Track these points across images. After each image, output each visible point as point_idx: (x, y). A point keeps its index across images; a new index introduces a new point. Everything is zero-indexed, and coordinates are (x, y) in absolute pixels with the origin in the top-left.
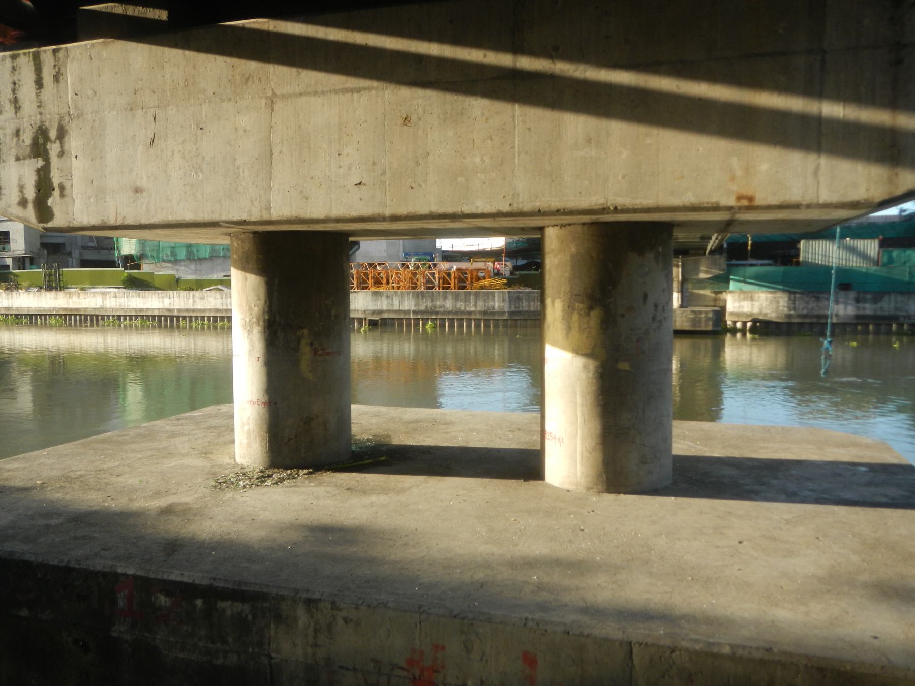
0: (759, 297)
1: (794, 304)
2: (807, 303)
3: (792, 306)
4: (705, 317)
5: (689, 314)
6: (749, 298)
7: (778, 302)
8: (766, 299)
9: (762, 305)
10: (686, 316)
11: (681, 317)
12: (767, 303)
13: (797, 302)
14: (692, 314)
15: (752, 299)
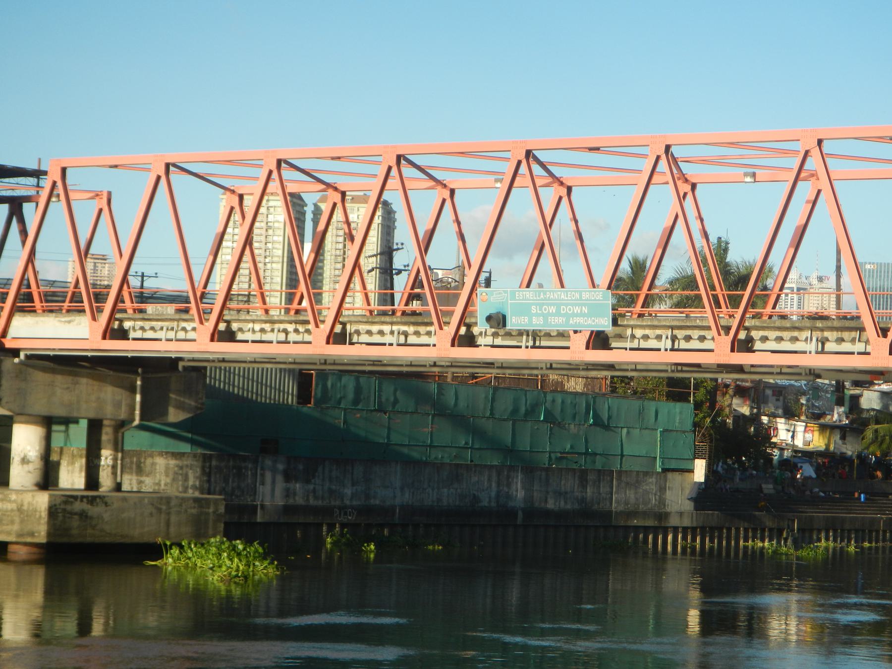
0: (153, 464)
1: (209, 481)
2: (226, 481)
3: (206, 486)
4: (214, 512)
5: (191, 508)
6: (134, 466)
7: (186, 479)
8: (167, 468)
9: (159, 484)
10: (186, 511)
11: (179, 513)
12: (168, 480)
13: (212, 480)
14: (194, 508)
15: (140, 471)
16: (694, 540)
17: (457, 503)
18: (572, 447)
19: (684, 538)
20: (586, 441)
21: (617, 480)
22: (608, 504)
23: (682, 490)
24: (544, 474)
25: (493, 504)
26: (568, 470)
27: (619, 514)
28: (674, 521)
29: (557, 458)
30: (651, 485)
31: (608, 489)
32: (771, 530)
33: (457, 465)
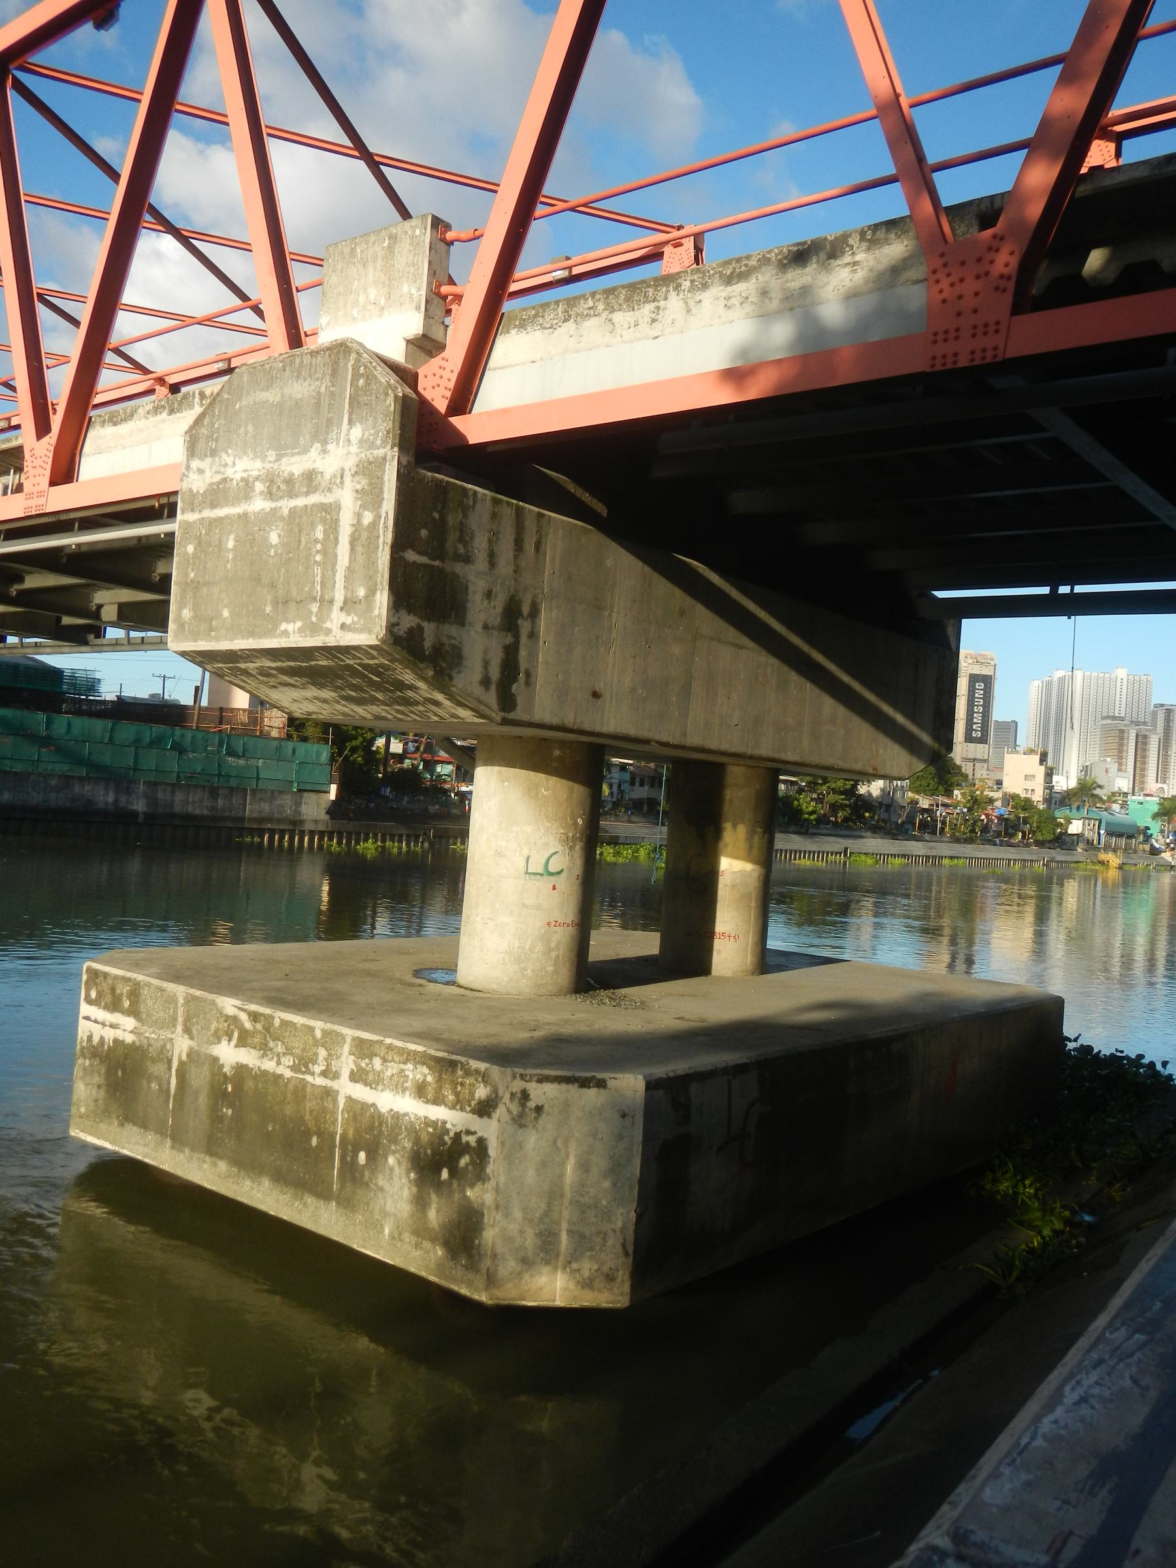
16: (281, 839)
17: (68, 805)
18: (202, 770)
19: (321, 839)
20: (219, 765)
21: (250, 795)
22: (241, 812)
23: (318, 806)
24: (169, 788)
25: (110, 807)
26: (197, 786)
27: (249, 819)
28: (308, 826)
29: (186, 777)
30: (286, 801)
31: (241, 802)
32: (408, 836)
33: (69, 776)
